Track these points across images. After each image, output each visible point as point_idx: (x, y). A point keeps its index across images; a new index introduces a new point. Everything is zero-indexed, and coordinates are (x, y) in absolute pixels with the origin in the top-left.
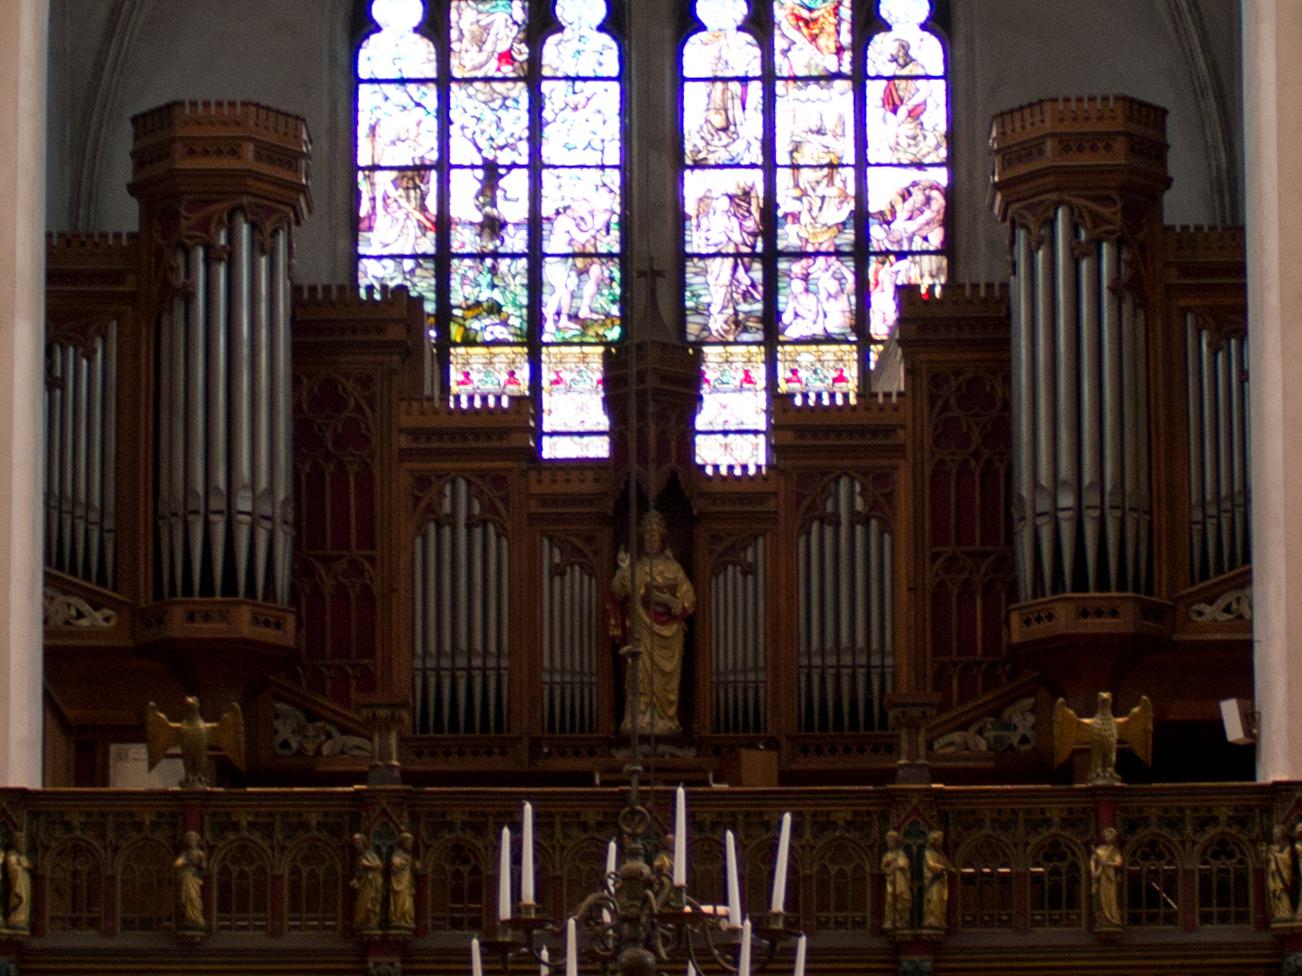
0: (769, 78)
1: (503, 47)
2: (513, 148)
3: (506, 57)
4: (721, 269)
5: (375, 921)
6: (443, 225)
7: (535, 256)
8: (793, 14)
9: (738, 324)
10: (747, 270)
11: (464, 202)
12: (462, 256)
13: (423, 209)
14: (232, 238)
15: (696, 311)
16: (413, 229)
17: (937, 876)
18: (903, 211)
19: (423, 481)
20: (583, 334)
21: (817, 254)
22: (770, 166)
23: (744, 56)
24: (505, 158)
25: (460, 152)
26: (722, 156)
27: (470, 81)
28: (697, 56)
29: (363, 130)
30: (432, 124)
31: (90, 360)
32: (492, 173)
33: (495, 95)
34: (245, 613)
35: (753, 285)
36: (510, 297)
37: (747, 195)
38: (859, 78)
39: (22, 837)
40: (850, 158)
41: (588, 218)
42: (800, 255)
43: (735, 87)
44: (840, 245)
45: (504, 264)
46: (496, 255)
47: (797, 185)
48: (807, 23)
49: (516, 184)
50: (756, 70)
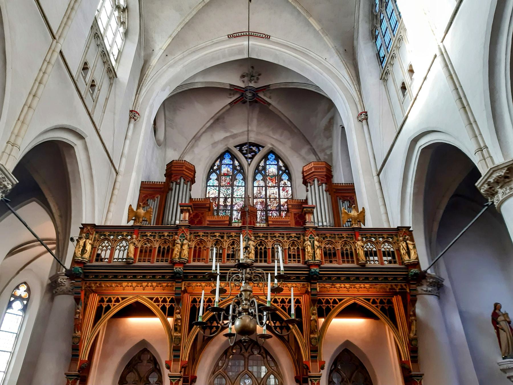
3: (229, 183)
11: (221, 203)
21: (273, 210)
25: (221, 195)
27: (223, 186)
35: (264, 214)
40: (278, 197)
43: (261, 188)
48: (271, 179)
49: (229, 200)
50: (264, 185)
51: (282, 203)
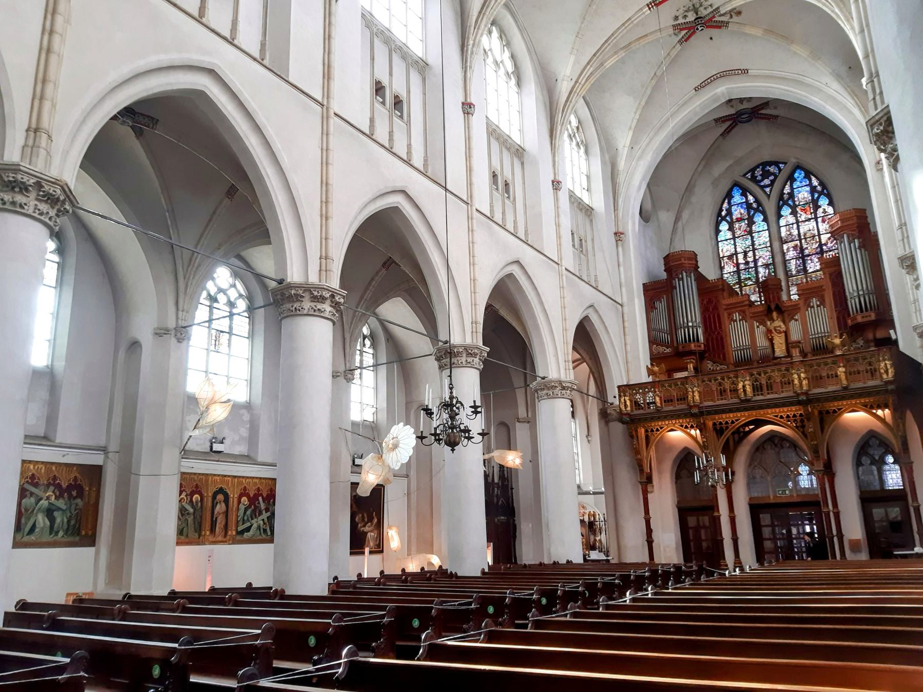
0: (797, 222)
3: (745, 231)
4: (793, 262)
5: (692, 402)
6: (738, 265)
7: (756, 267)
9: (798, 272)
11: (741, 260)
13: (733, 263)
14: (682, 276)
15: (789, 271)
16: (732, 267)
17: (804, 379)
18: (829, 242)
19: (729, 314)
22: (800, 240)
23: (791, 219)
24: (748, 250)
25: (739, 250)
26: (790, 239)
28: (782, 222)
29: (720, 251)
30: (733, 246)
31: (661, 303)
32: (745, 253)
34: (693, 345)
37: (796, 246)
38: (816, 218)
39: (627, 394)
42: (808, 255)
43: (791, 226)
45: (750, 270)
46: (749, 268)
49: (750, 254)
51: (823, 242)
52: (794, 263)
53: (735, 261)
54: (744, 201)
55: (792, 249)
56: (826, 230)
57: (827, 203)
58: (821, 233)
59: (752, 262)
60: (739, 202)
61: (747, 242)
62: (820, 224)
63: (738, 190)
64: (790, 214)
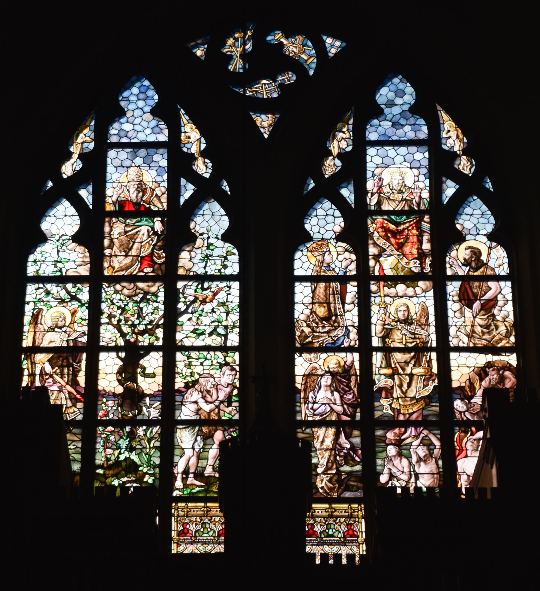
1: (145, 252)
2: (151, 332)
8: (382, 227)
10: (348, 437)
12: (106, 424)
13: (74, 383)
20: (207, 491)
21: (407, 424)
24: (145, 341)
26: (326, 340)
30: (83, 313)
33: (138, 291)
36: (145, 458)
41: (214, 391)
44: (428, 415)
47: (388, 365)
50: (352, 269)
52: (329, 442)
53: (81, 379)
54: (163, 137)
55: (326, 380)
56: (470, 336)
57: (490, 228)
58: (453, 342)
59: (152, 396)
60: (141, 137)
61: (147, 309)
62: (453, 307)
63: (143, 91)
64: (339, 238)
